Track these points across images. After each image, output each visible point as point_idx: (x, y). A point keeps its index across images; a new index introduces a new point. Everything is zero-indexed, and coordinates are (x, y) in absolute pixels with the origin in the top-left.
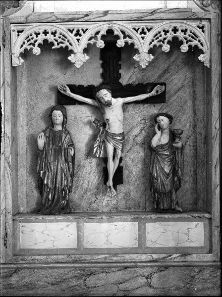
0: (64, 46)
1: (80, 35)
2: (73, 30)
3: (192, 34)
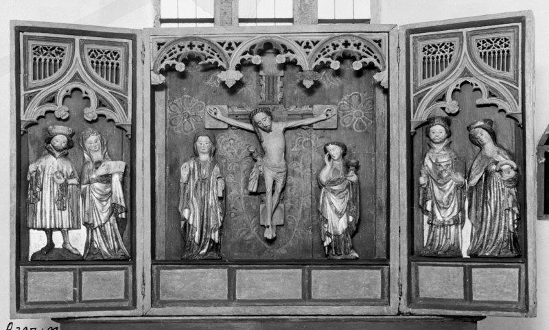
0: (213, 61)
1: (233, 49)
2: (224, 43)
3: (366, 49)
